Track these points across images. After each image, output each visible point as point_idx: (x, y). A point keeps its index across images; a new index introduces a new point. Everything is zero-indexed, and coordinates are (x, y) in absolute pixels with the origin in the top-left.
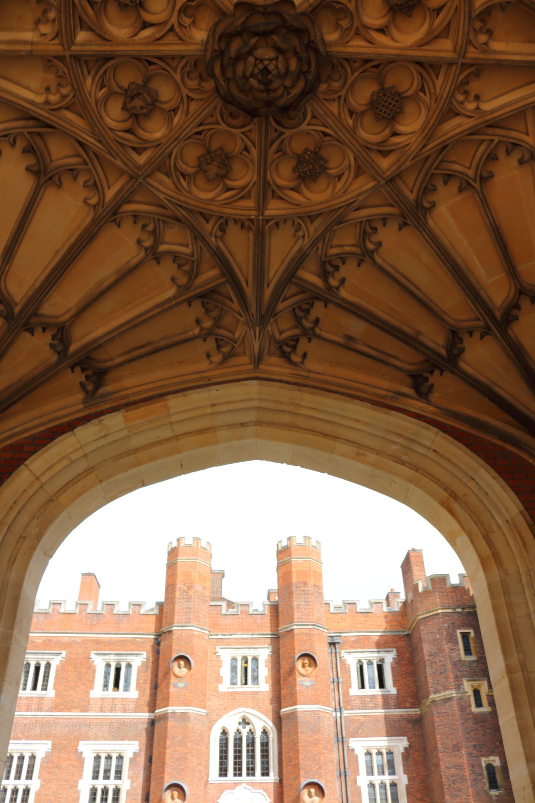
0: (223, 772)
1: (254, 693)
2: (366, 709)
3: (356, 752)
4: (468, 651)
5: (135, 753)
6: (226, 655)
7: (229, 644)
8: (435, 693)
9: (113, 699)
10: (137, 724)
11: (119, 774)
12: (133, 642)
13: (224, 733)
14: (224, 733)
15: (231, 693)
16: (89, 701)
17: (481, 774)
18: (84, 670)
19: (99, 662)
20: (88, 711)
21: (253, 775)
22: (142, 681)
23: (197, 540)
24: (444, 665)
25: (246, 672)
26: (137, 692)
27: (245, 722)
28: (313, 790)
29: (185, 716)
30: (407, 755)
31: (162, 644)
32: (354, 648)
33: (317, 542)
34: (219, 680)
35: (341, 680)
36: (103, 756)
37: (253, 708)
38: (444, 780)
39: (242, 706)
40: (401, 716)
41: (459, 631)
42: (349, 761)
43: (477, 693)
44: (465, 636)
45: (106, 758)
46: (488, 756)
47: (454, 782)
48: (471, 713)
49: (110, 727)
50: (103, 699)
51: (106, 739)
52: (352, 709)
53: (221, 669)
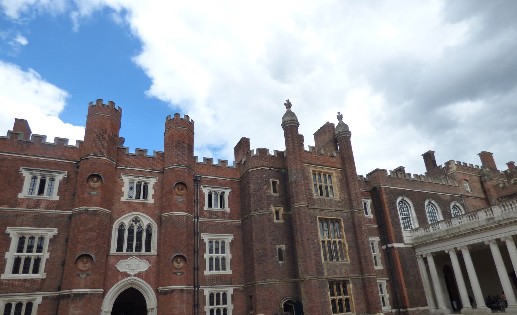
0: (120, 248)
1: (144, 204)
2: (212, 218)
3: (205, 241)
4: (275, 191)
5: (54, 236)
6: (126, 179)
7: (130, 173)
8: (255, 211)
9: (38, 200)
10: (57, 218)
11: (40, 249)
12: (57, 164)
13: (122, 225)
14: (122, 225)
15: (129, 202)
16: (17, 200)
17: (276, 253)
18: (13, 179)
19: (27, 175)
20: (15, 207)
21: (140, 251)
22: (62, 190)
23: (113, 103)
24: (262, 197)
25: (141, 190)
27: (136, 220)
28: (179, 260)
30: (232, 244)
31: (81, 166)
32: (208, 184)
33: (192, 120)
34: (122, 194)
35: (199, 201)
37: (143, 213)
38: (255, 256)
39: (135, 211)
40: (231, 223)
41: (271, 180)
42: (200, 245)
43: (277, 212)
44: (274, 183)
46: (280, 244)
47: (261, 257)
48: (274, 223)
49: (34, 218)
50: (29, 200)
51: (31, 226)
52: (204, 218)
53: (123, 188)
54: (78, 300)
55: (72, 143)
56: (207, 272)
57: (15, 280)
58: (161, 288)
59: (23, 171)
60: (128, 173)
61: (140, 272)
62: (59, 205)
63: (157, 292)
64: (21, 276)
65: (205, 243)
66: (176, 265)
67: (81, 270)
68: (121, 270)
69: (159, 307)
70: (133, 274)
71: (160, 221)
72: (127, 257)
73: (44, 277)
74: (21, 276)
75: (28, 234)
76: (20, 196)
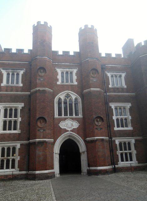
0: (60, 114)
5: (22, 107)
11: (16, 116)
13: (60, 99)
22: (24, 80)
26: (22, 84)
29: (44, 91)
30: (131, 109)
32: (110, 70)
34: (57, 80)
36: (8, 109)
37: (71, 91)
39: (66, 90)
40: (129, 95)
45: (10, 110)
51: (9, 102)
52: (110, 92)
54: (40, 146)
55: (26, 51)
56: (116, 129)
57: (5, 134)
58: (88, 139)
59: (2, 70)
60: (60, 67)
61: (74, 129)
62: (23, 89)
63: (85, 141)
64: (8, 132)
65: (112, 109)
66: (97, 123)
67: (40, 127)
68: (62, 128)
69: (87, 151)
70: (69, 130)
71: (83, 96)
72: (65, 119)
73: (20, 132)
74: (8, 132)
75: (9, 107)
76: (2, 85)
